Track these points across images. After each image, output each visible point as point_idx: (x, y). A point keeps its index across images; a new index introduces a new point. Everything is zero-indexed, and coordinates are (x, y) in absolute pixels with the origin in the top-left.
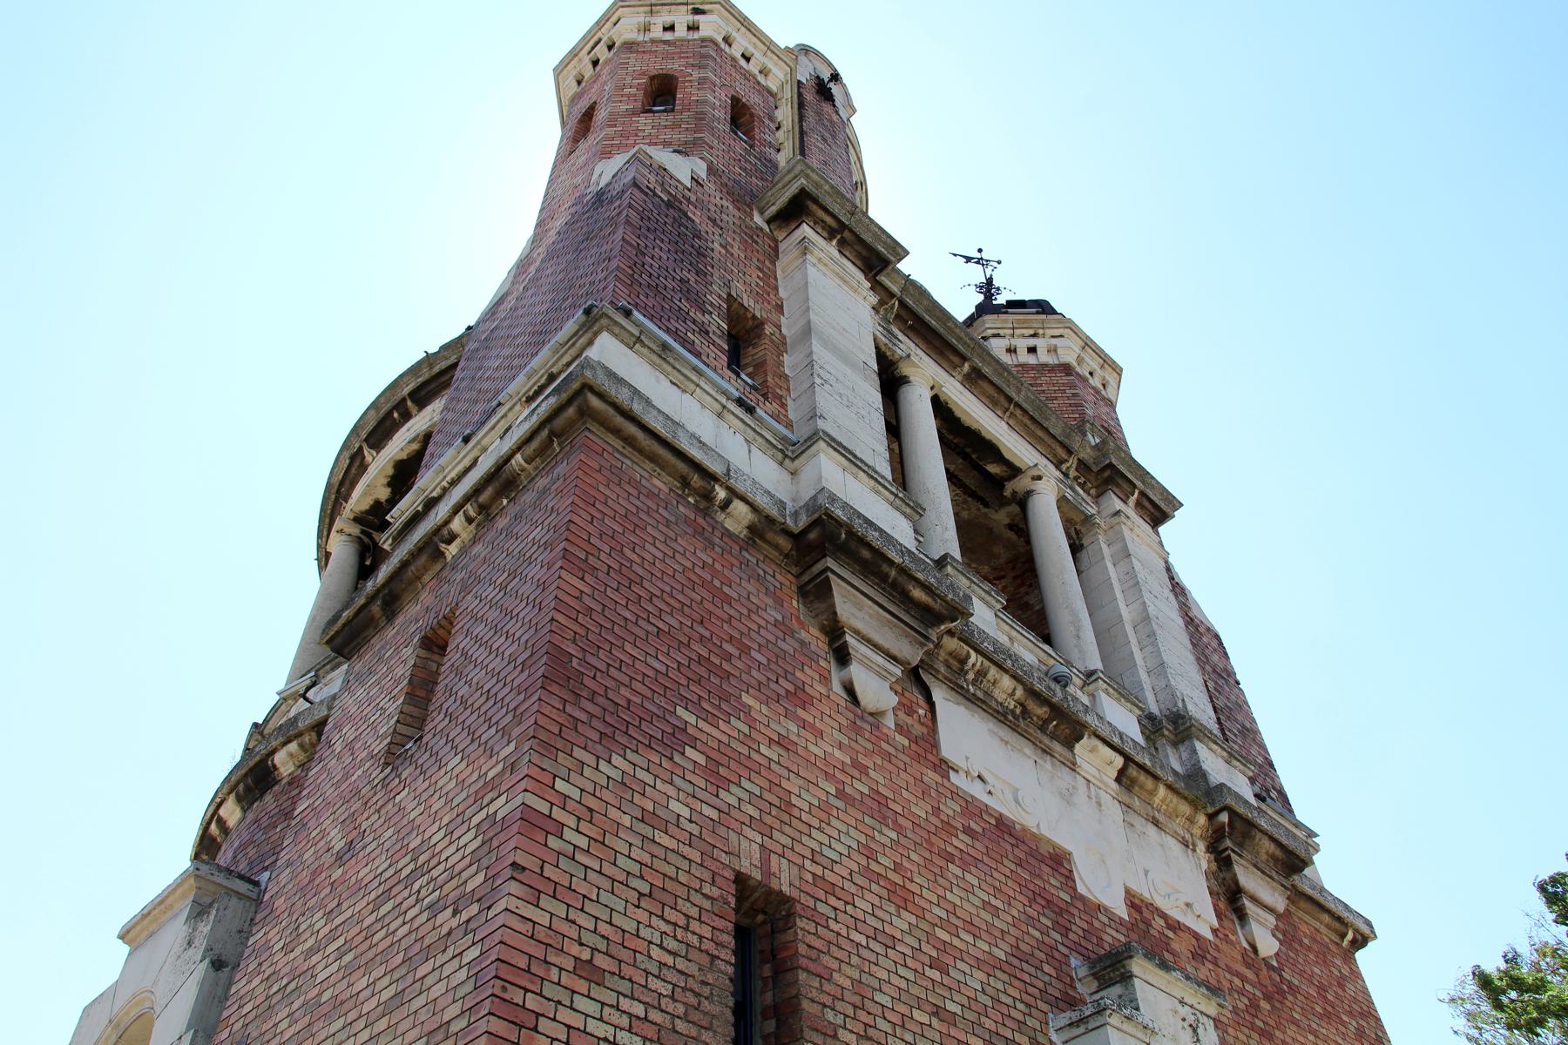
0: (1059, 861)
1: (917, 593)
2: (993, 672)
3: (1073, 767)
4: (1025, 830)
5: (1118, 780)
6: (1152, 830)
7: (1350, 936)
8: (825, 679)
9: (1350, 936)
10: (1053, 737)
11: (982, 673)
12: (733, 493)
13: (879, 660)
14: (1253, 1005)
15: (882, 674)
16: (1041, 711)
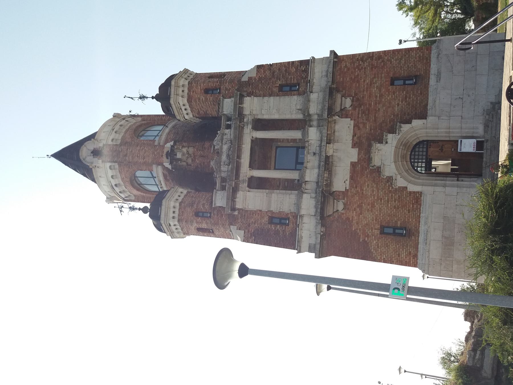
0: (353, 165)
1: (323, 200)
2: (325, 179)
3: (332, 156)
4: (350, 173)
5: (330, 144)
6: (337, 134)
7: (335, 60)
8: (343, 214)
9: (335, 60)
10: (329, 161)
11: (326, 180)
12: (321, 232)
13: (335, 204)
14: (363, 112)
15: (337, 204)
16: (326, 166)
